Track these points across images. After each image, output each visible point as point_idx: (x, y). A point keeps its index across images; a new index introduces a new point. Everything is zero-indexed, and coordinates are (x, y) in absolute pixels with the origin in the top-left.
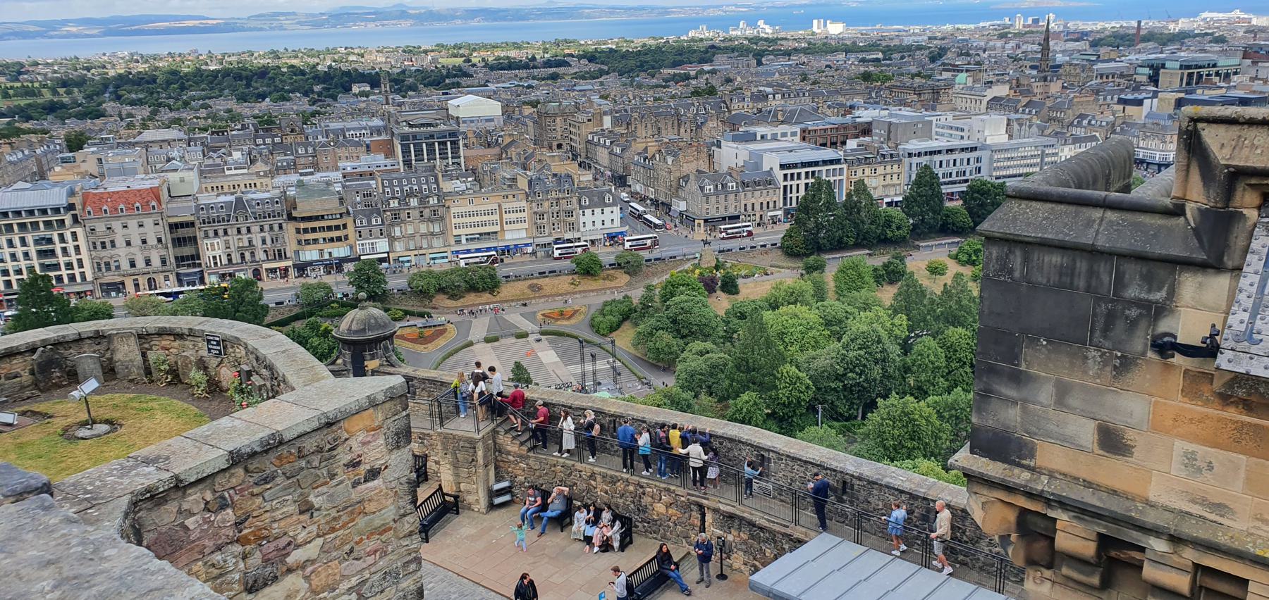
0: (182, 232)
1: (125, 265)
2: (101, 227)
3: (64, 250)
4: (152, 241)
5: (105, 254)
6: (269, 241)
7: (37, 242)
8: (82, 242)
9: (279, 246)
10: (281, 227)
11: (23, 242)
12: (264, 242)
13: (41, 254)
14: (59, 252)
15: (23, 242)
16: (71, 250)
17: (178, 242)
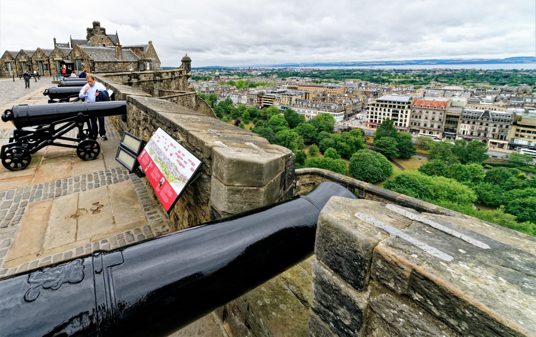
0: (451, 119)
1: (422, 125)
2: (417, 111)
3: (401, 116)
4: (437, 119)
5: (416, 120)
6: (497, 131)
7: (393, 111)
8: (409, 115)
9: (502, 134)
10: (507, 127)
11: (389, 111)
12: (494, 130)
13: (393, 115)
14: (399, 116)
15: (389, 111)
16: (404, 116)
17: (448, 122)
